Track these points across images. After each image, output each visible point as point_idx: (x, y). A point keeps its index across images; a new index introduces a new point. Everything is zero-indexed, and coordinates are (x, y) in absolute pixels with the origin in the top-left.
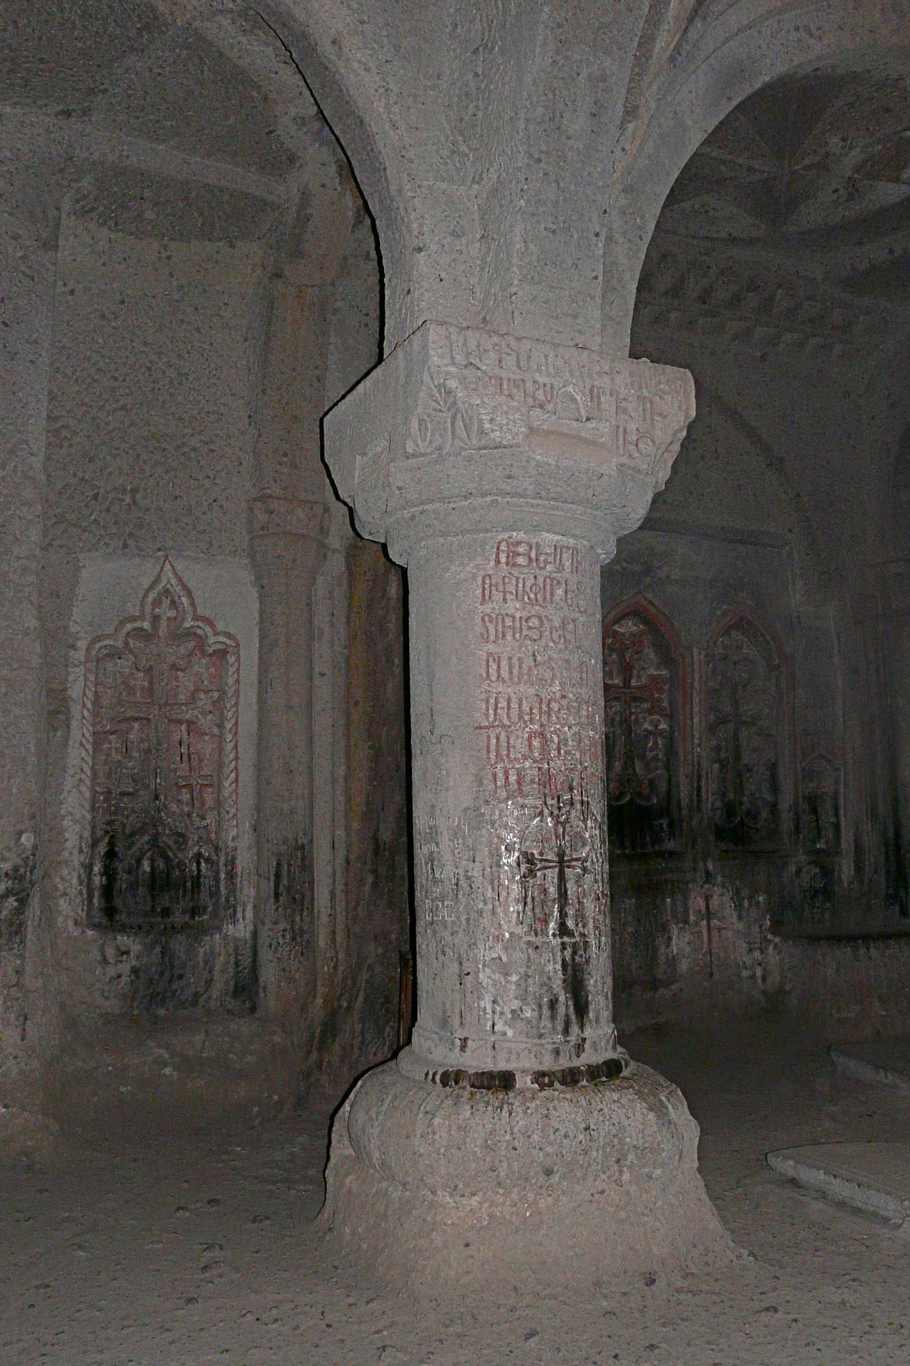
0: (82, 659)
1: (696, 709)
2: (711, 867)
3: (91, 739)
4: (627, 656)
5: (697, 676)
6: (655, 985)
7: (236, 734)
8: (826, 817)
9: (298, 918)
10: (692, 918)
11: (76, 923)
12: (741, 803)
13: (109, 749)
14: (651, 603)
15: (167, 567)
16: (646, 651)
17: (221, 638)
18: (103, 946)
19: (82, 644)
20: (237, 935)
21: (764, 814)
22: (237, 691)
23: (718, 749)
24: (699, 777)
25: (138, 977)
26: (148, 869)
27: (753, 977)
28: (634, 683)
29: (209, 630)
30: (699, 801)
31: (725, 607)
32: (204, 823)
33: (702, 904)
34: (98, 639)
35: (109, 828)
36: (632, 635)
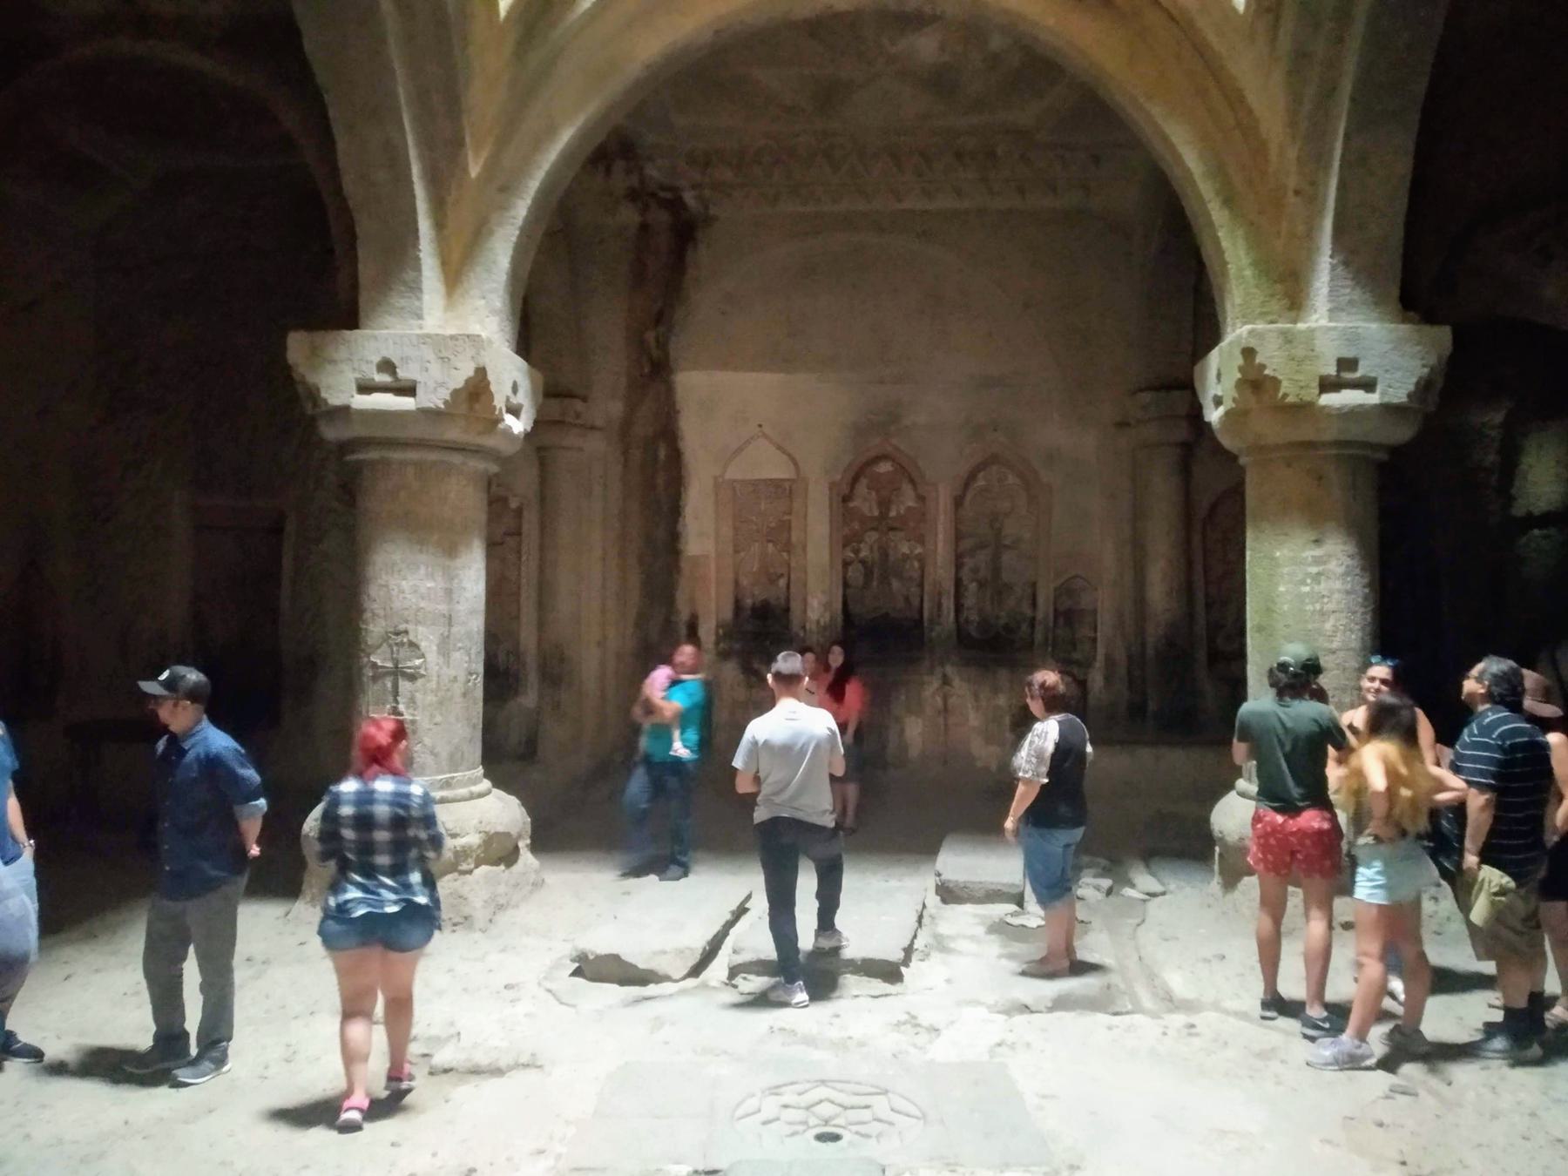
1: (941, 536)
12: (998, 617)
21: (1024, 627)
23: (975, 570)
24: (940, 594)
28: (893, 514)
33: (939, 699)
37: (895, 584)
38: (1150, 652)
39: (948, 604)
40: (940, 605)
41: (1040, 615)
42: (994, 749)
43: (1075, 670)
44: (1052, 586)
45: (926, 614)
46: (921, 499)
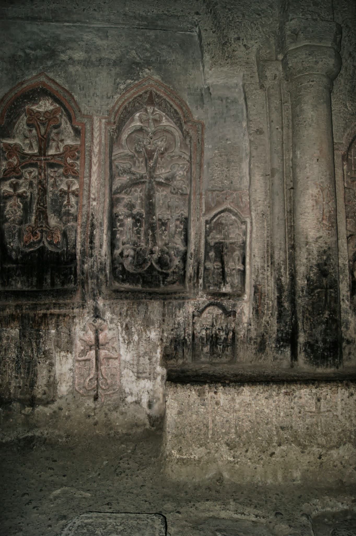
1: (94, 168)
2: (101, 303)
4: (43, 130)
5: (96, 141)
6: (33, 402)
8: (233, 265)
10: (79, 346)
12: (152, 252)
14: (54, 81)
16: (63, 125)
21: (177, 261)
23: (131, 206)
24: (93, 226)
27: (137, 403)
28: (52, 152)
30: (92, 248)
31: (129, 81)
33: (91, 335)
36: (47, 112)
37: (53, 221)
38: (301, 282)
39: (102, 236)
40: (92, 237)
41: (192, 248)
42: (147, 384)
43: (225, 303)
44: (203, 220)
45: (79, 247)
46: (77, 132)
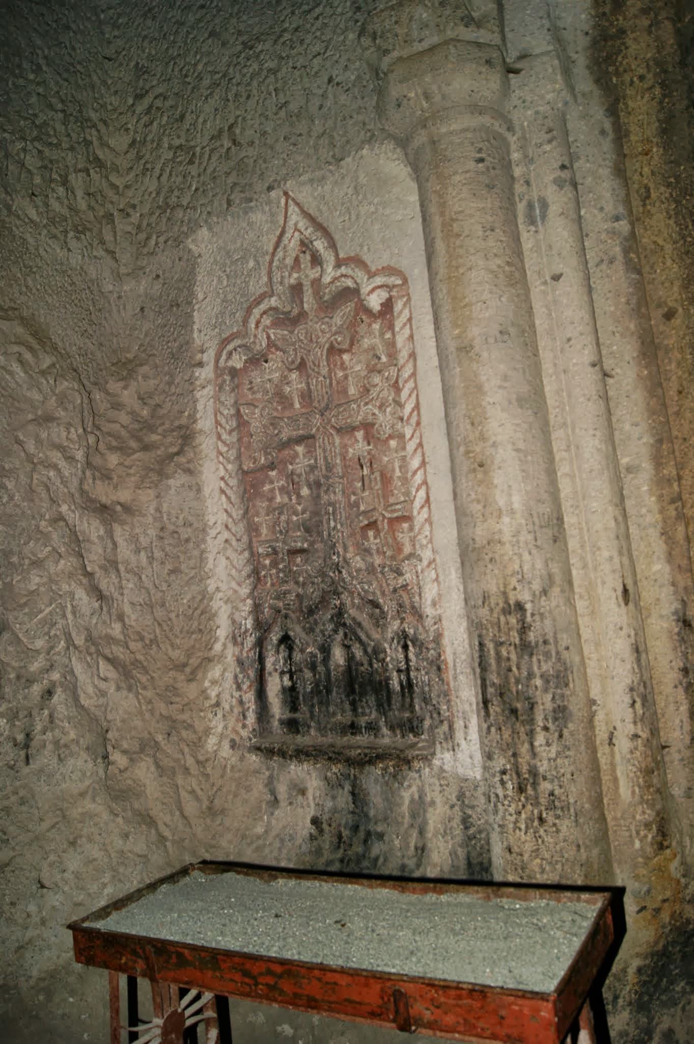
0: (212, 375)
3: (233, 482)
7: (418, 424)
9: (524, 749)
11: (233, 745)
13: (272, 490)
15: (292, 208)
17: (379, 280)
18: (271, 777)
19: (209, 357)
20: (460, 771)
22: (413, 355)
25: (321, 831)
26: (342, 662)
29: (360, 275)
32: (401, 581)
34: (225, 342)
35: (281, 604)
